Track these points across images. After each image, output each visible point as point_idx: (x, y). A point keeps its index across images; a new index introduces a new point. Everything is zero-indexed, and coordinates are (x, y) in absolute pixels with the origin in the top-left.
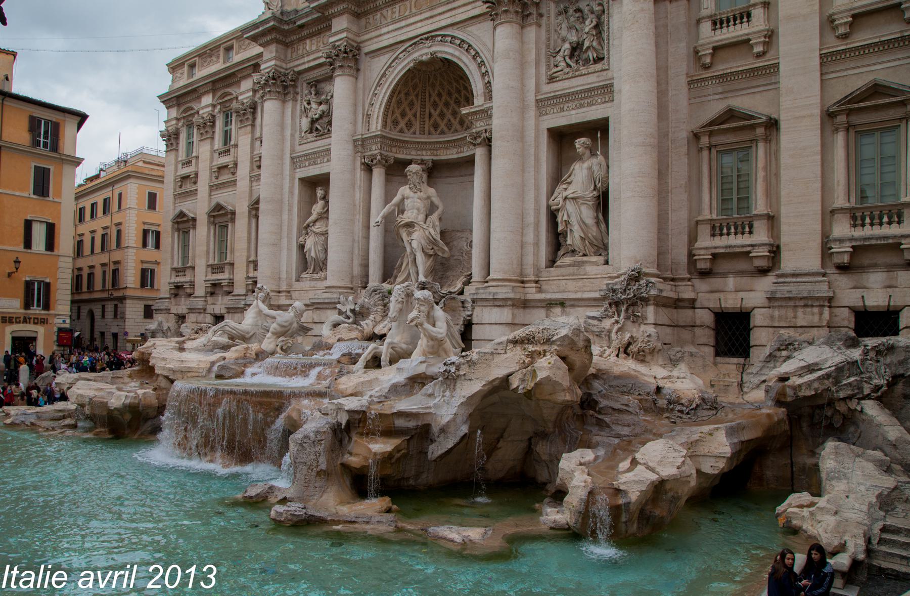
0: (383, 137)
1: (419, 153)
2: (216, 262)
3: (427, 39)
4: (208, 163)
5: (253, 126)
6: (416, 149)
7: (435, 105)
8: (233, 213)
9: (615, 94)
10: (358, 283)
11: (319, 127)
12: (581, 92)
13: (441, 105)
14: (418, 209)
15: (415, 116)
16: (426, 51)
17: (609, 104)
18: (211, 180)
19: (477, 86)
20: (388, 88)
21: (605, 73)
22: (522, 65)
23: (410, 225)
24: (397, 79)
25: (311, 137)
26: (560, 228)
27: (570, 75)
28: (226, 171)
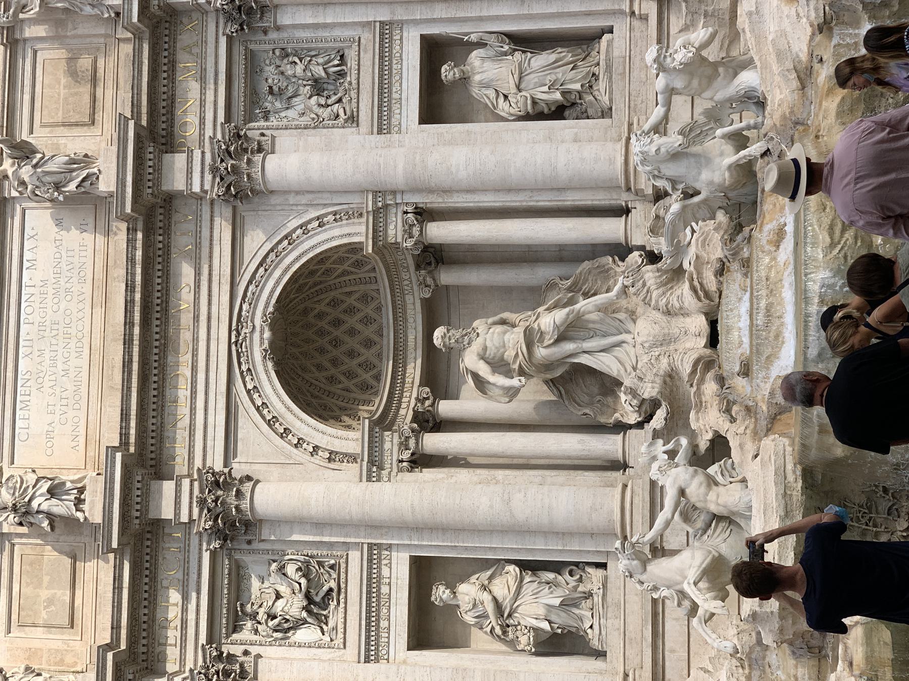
1: (404, 405)
3: (239, 334)
6: (398, 408)
7: (332, 379)
9: (396, 18)
10: (618, 475)
12: (381, 70)
13: (333, 371)
14: (505, 333)
16: (256, 336)
17: (405, 34)
19: (335, 236)
21: (362, 41)
23: (531, 338)
25: (335, 618)
26: (558, 96)
27: (353, 94)
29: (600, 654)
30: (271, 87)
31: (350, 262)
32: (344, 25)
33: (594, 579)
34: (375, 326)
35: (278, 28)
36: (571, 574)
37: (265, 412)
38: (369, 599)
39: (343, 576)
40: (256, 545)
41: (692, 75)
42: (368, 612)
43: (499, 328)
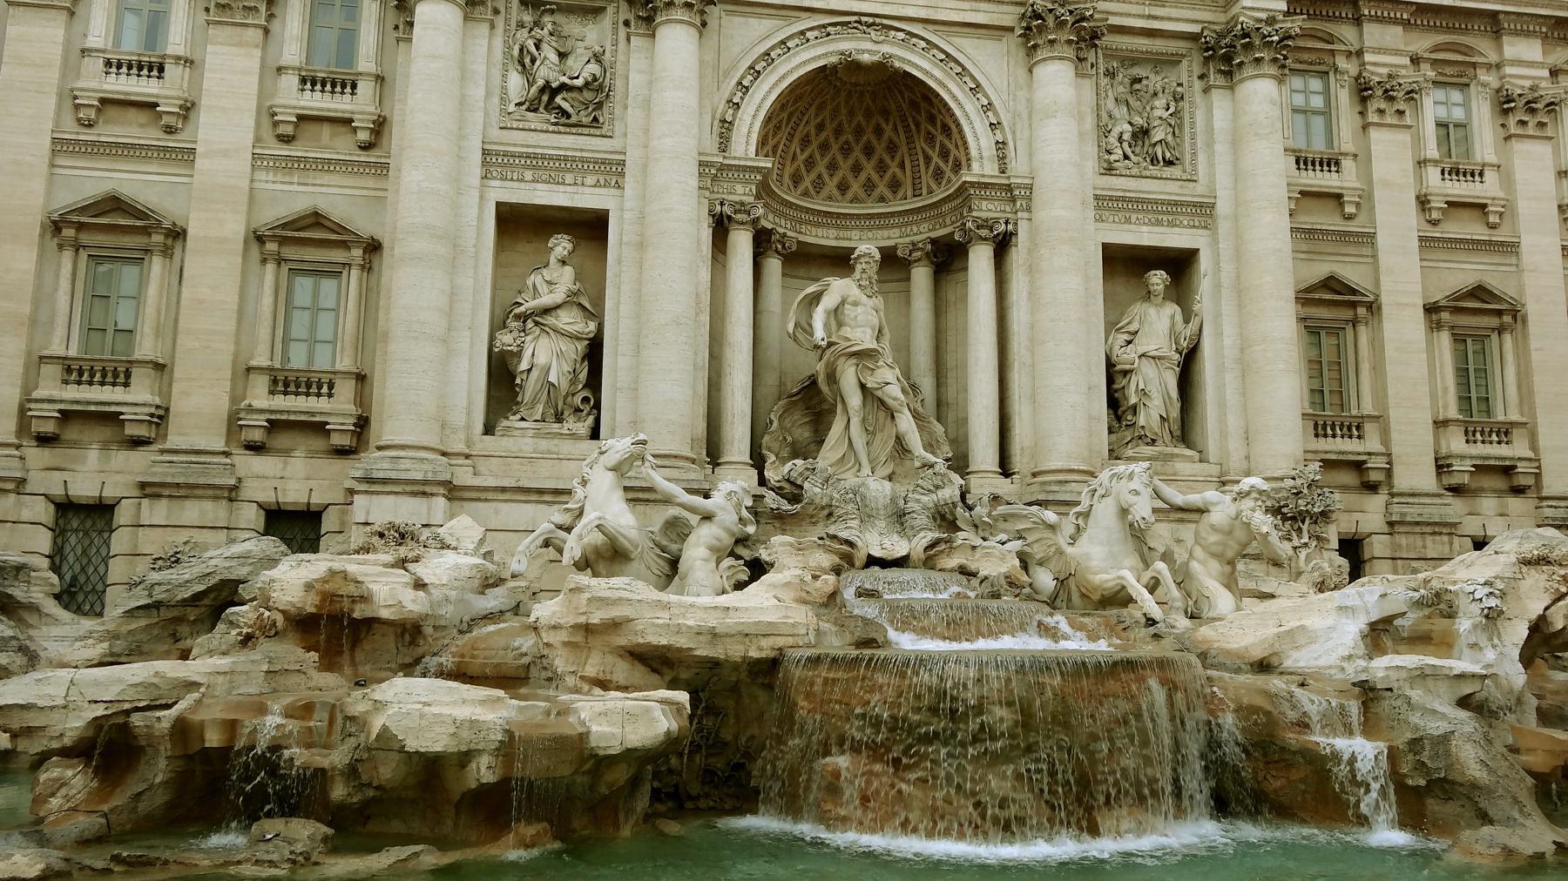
0: (765, 173)
2: (73, 352)
4: (54, 75)
5: (266, 31)
7: (806, 142)
8: (177, 234)
11: (566, 106)
13: (815, 145)
15: (775, 148)
17: (1200, 231)
18: (57, 123)
19: (978, 139)
20: (776, 84)
21: (1191, 185)
22: (1081, 134)
24: (796, 76)
25: (536, 120)
26: (1133, 400)
27: (1135, 171)
28: (132, 114)
29: (489, 430)
30: (1140, 80)
31: (941, 164)
32: (1211, 165)
33: (580, 425)
34: (862, 194)
35: (1206, 91)
36: (585, 400)
37: (779, 51)
38: (558, 158)
39: (586, 131)
40: (622, 31)
41: (1230, 533)
42: (543, 157)
43: (876, 322)
